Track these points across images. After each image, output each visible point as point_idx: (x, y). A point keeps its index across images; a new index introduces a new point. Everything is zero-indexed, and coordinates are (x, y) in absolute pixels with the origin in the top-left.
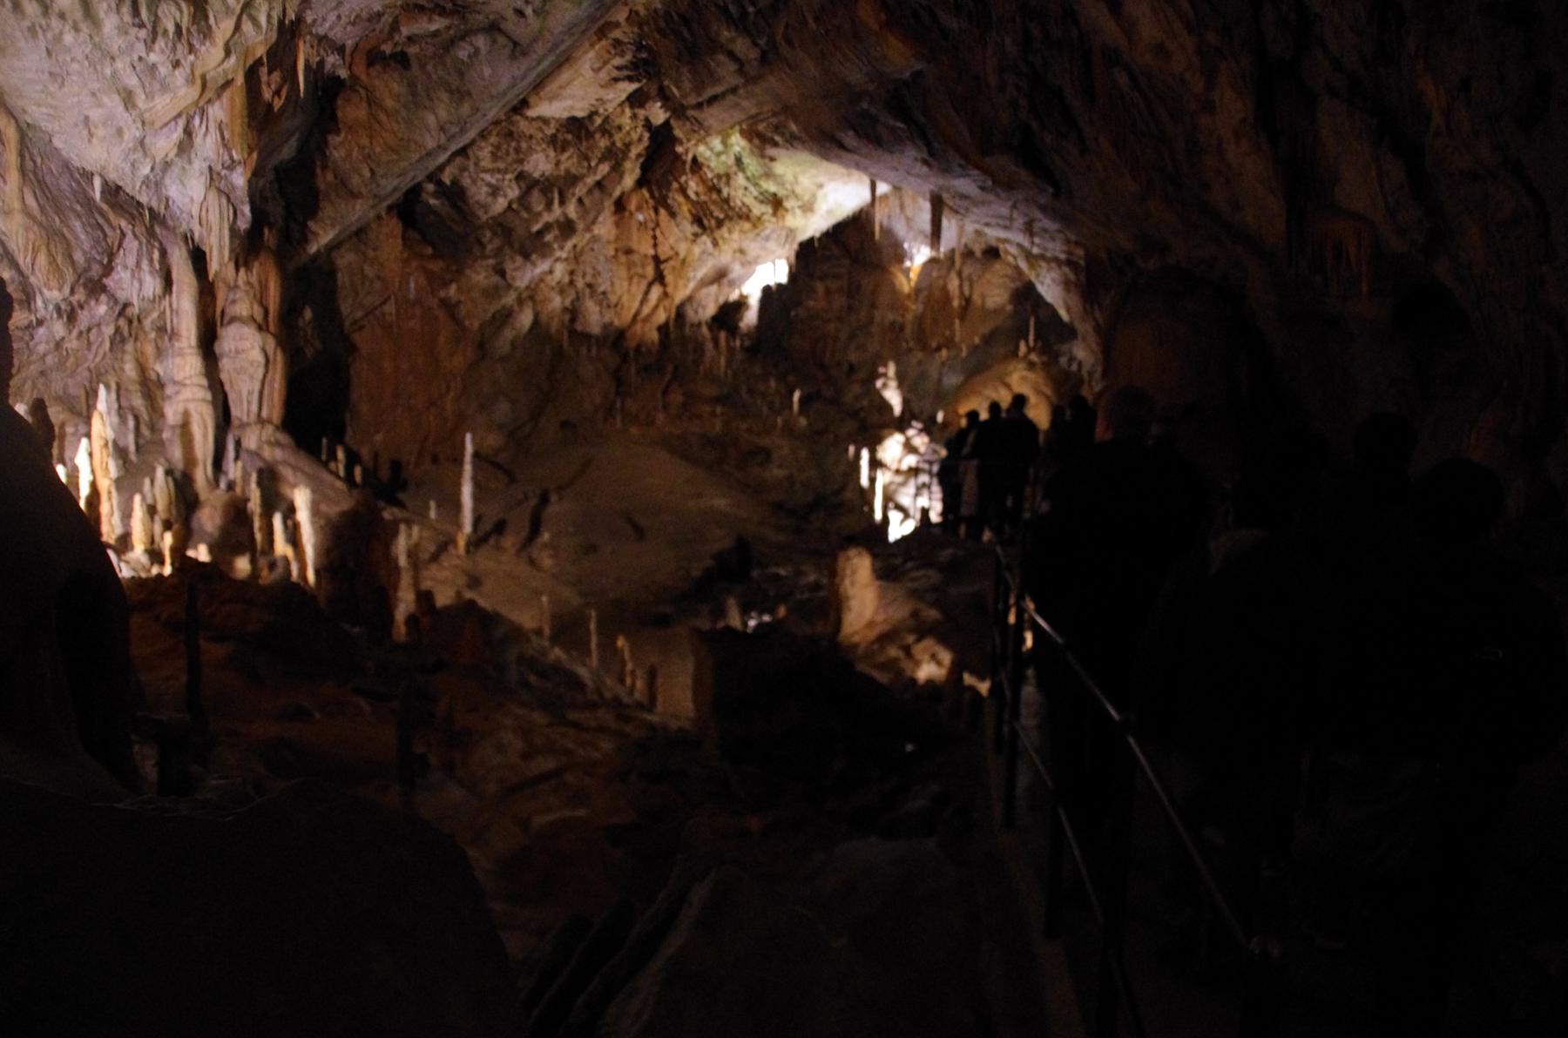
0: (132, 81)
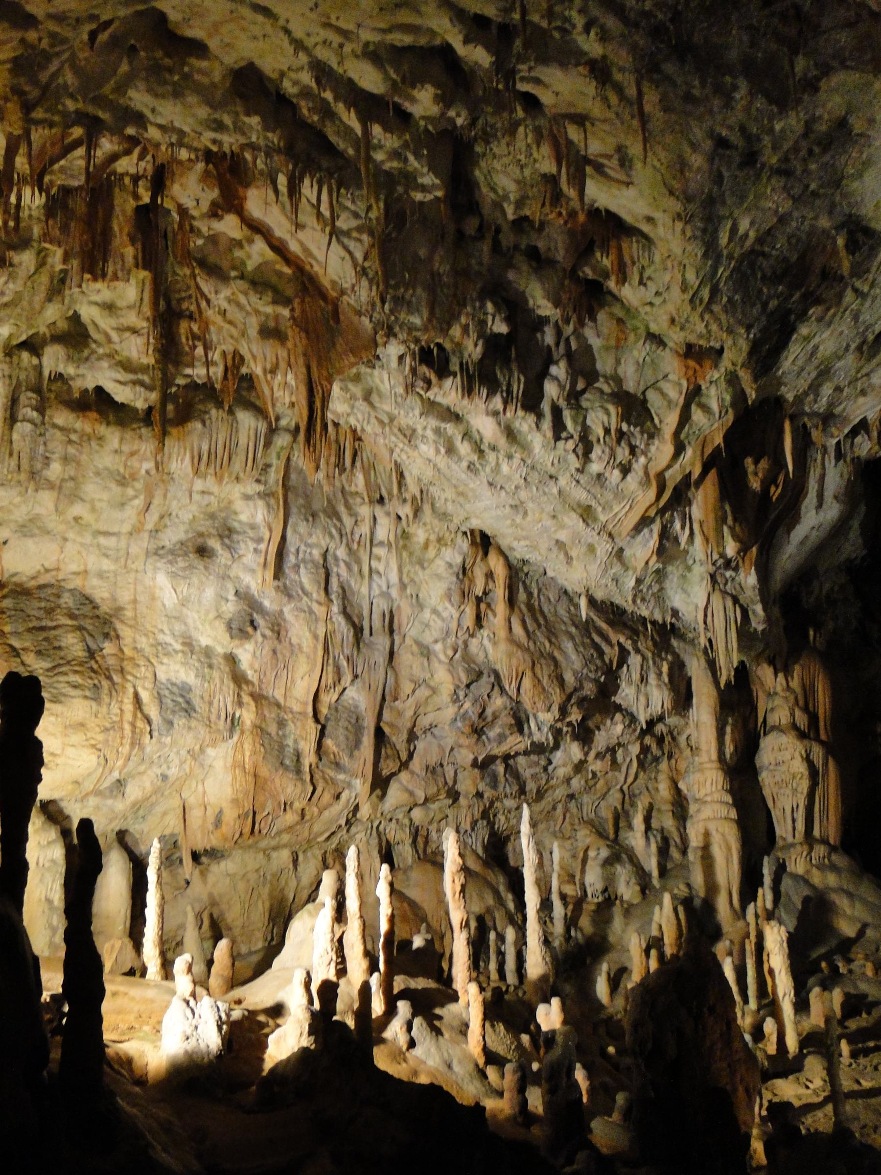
0: (580, 495)
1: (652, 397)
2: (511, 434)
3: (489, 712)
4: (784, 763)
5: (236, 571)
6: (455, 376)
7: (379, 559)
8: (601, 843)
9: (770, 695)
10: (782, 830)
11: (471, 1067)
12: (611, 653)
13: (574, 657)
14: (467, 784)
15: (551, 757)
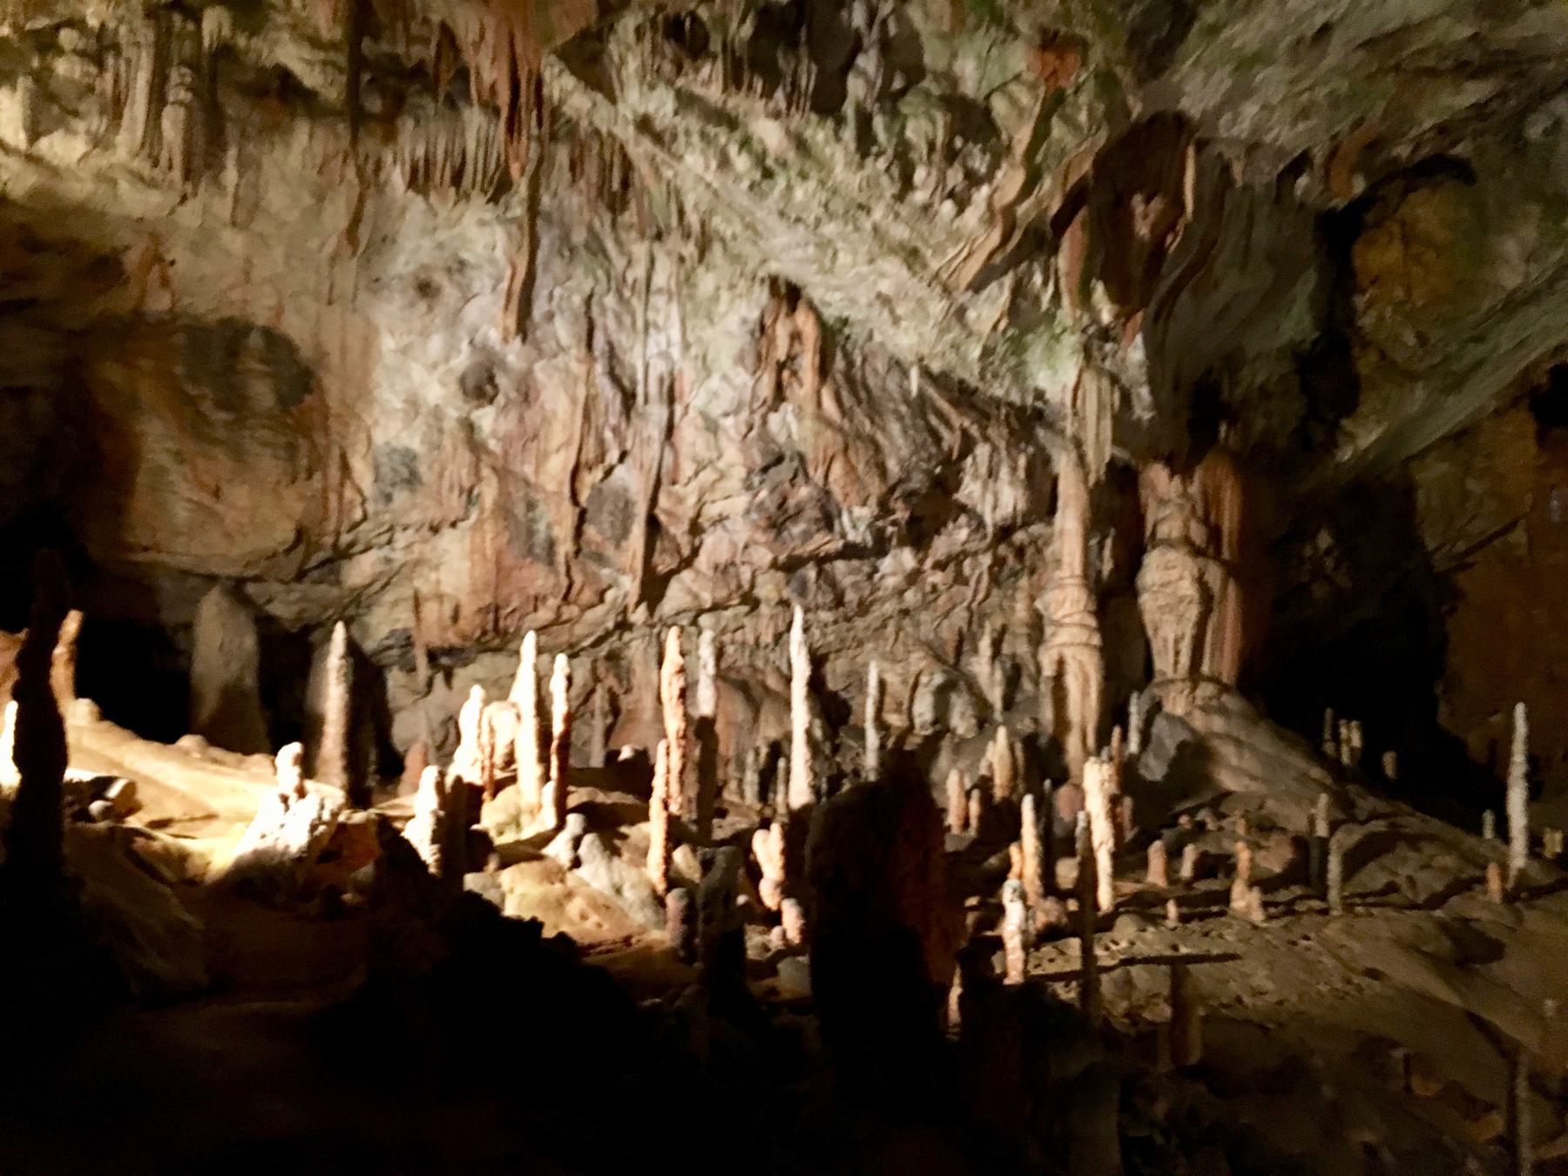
0: (900, 232)
1: (999, 106)
2: (801, 145)
3: (791, 502)
4: (1169, 585)
6: (715, 58)
7: (657, 311)
8: (937, 667)
9: (1162, 502)
10: (1163, 664)
11: (646, 893)
12: (951, 440)
13: (900, 441)
14: (768, 588)
15: (878, 563)
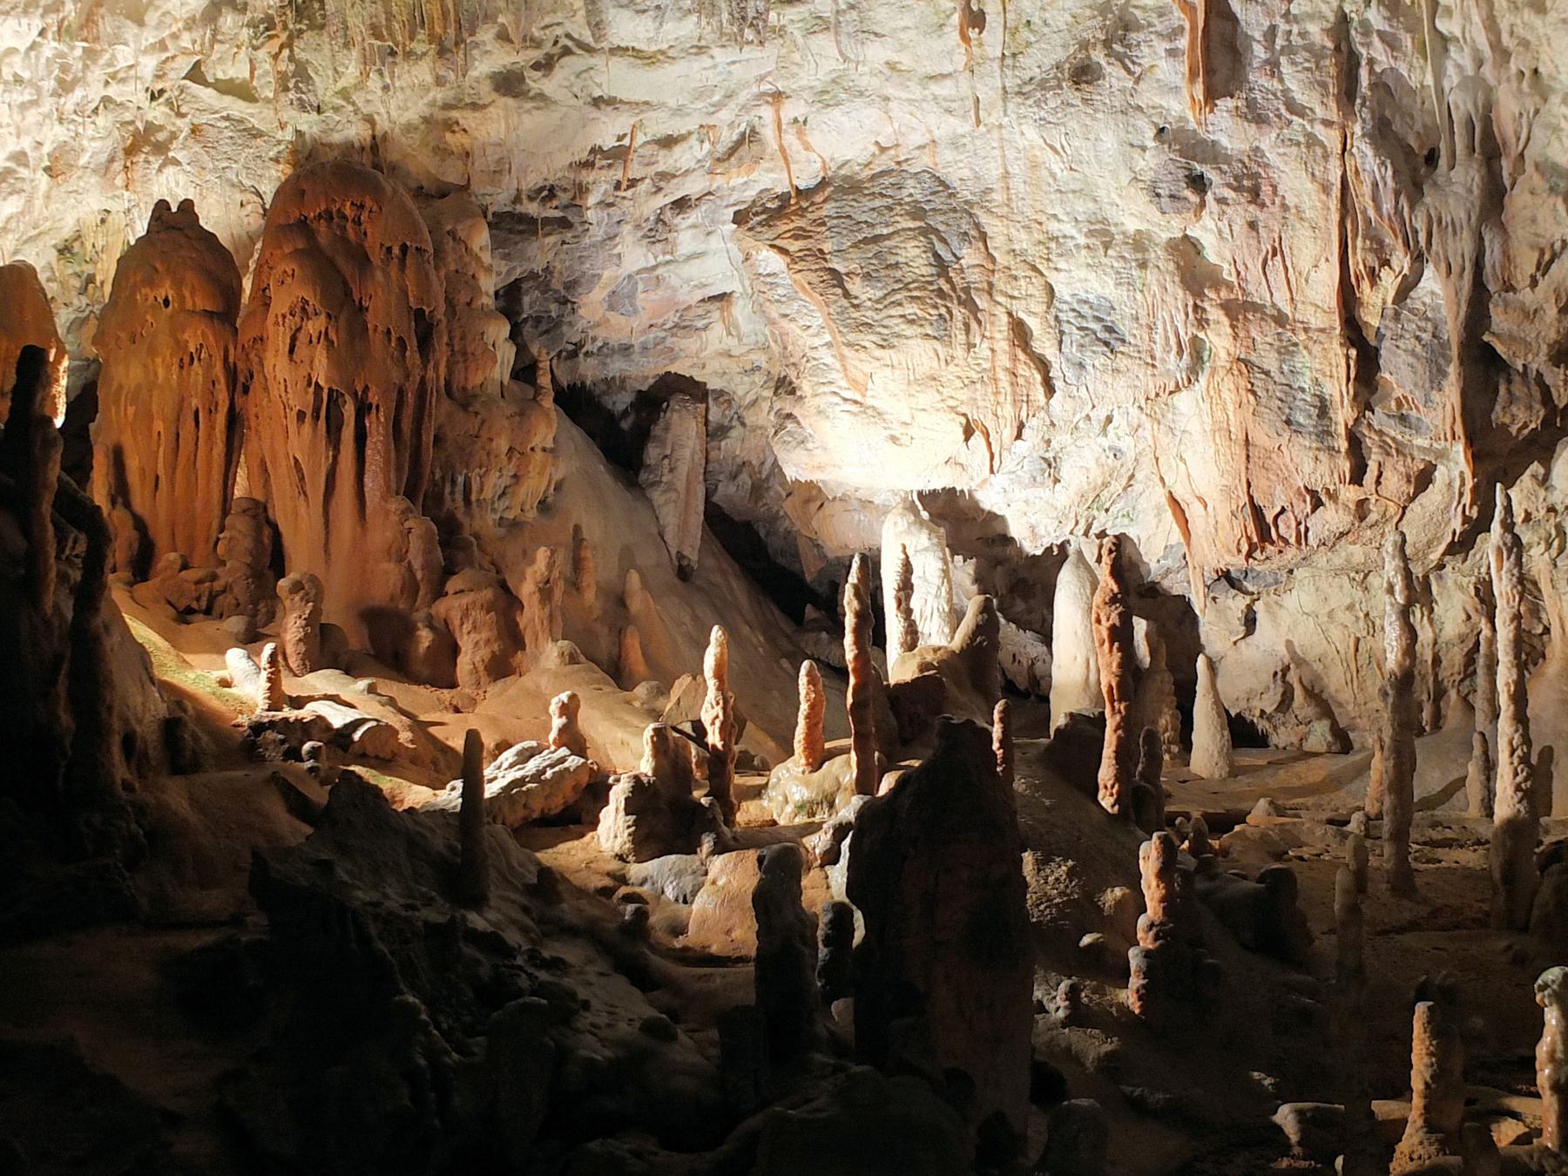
5: (1148, 96)
